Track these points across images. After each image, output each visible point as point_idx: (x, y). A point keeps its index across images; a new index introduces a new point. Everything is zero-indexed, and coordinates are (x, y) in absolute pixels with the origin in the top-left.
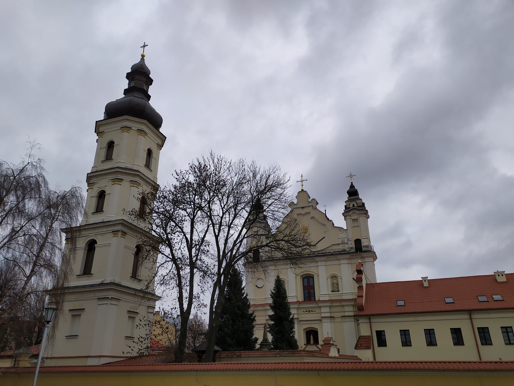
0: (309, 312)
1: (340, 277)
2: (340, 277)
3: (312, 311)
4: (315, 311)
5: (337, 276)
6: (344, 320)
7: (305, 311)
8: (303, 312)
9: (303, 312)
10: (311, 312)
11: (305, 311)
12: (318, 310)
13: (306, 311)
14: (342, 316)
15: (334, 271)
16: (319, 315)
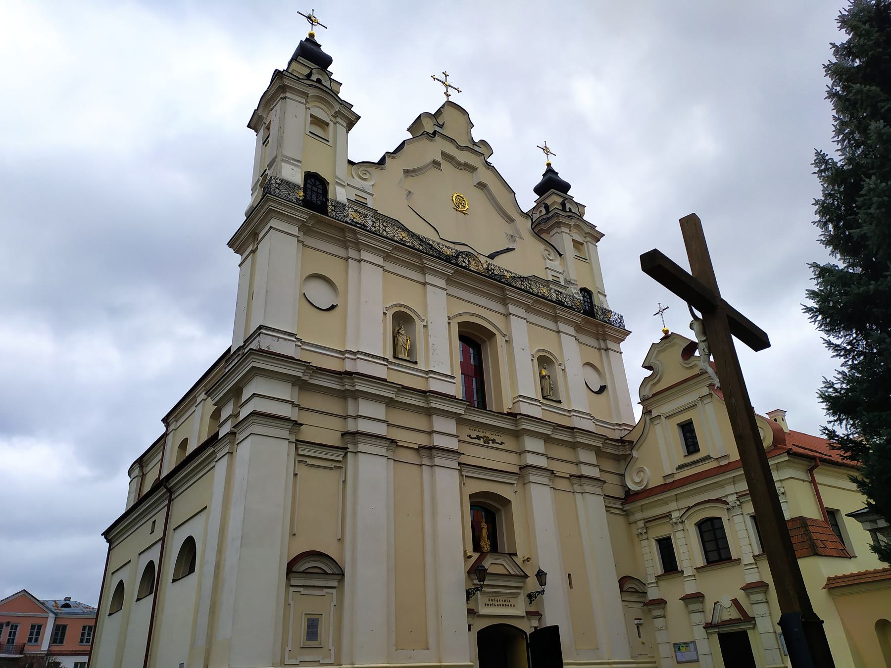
0: (485, 442)
1: (560, 365)
2: (560, 365)
3: (494, 441)
4: (502, 443)
5: (554, 360)
6: (577, 488)
7: (474, 434)
8: (470, 436)
9: (470, 436)
10: (491, 442)
11: (474, 434)
12: (509, 443)
13: (478, 438)
14: (571, 476)
15: (548, 343)
16: (513, 459)
